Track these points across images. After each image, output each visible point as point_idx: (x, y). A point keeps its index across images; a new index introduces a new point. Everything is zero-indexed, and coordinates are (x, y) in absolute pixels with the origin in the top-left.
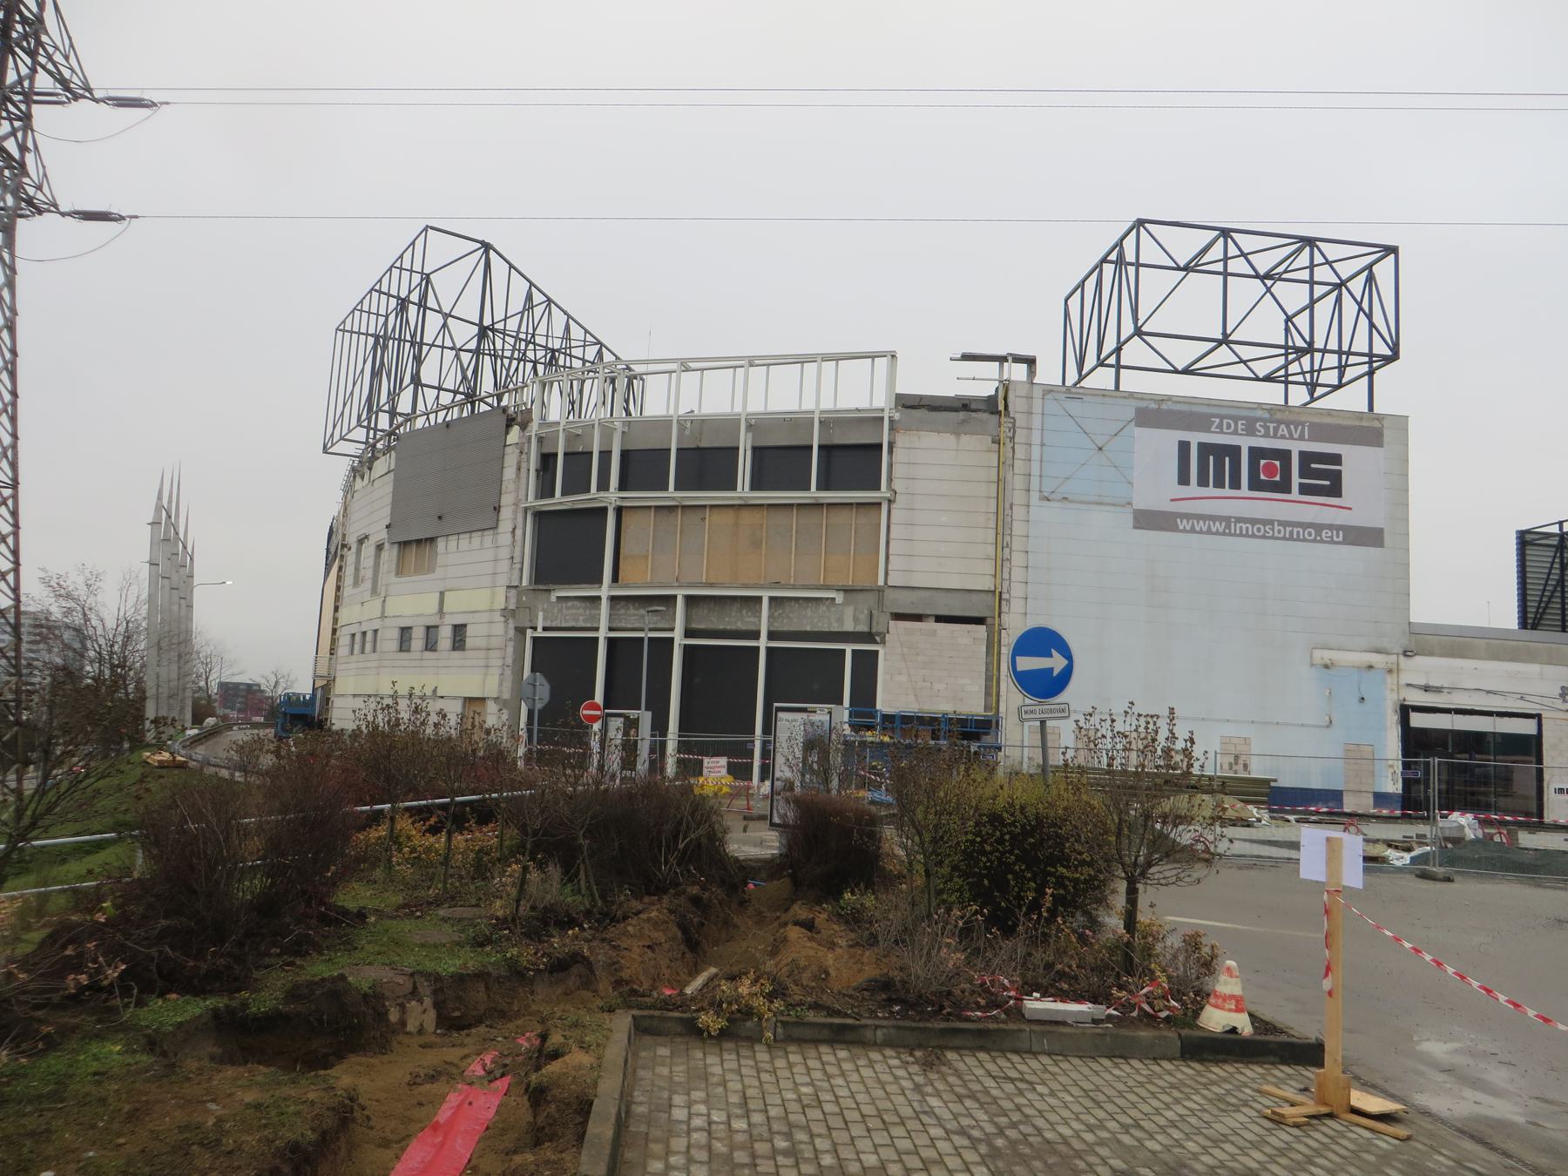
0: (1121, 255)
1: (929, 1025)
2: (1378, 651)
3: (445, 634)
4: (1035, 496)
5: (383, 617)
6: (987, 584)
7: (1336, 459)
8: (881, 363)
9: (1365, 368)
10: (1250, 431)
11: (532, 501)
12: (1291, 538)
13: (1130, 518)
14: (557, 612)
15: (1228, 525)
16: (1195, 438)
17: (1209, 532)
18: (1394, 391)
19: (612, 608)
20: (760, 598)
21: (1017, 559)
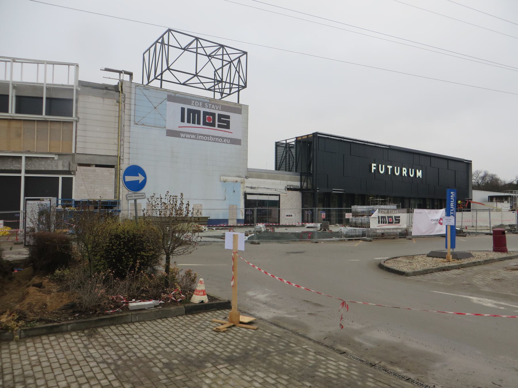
0: (163, 40)
1: (91, 319)
2: (239, 177)
4: (132, 123)
6: (115, 153)
7: (228, 117)
8: (72, 68)
9: (237, 89)
10: (204, 106)
12: (215, 141)
13: (165, 132)
15: (196, 136)
16: (186, 107)
17: (190, 138)
18: (245, 97)
20: (21, 157)
21: (126, 145)
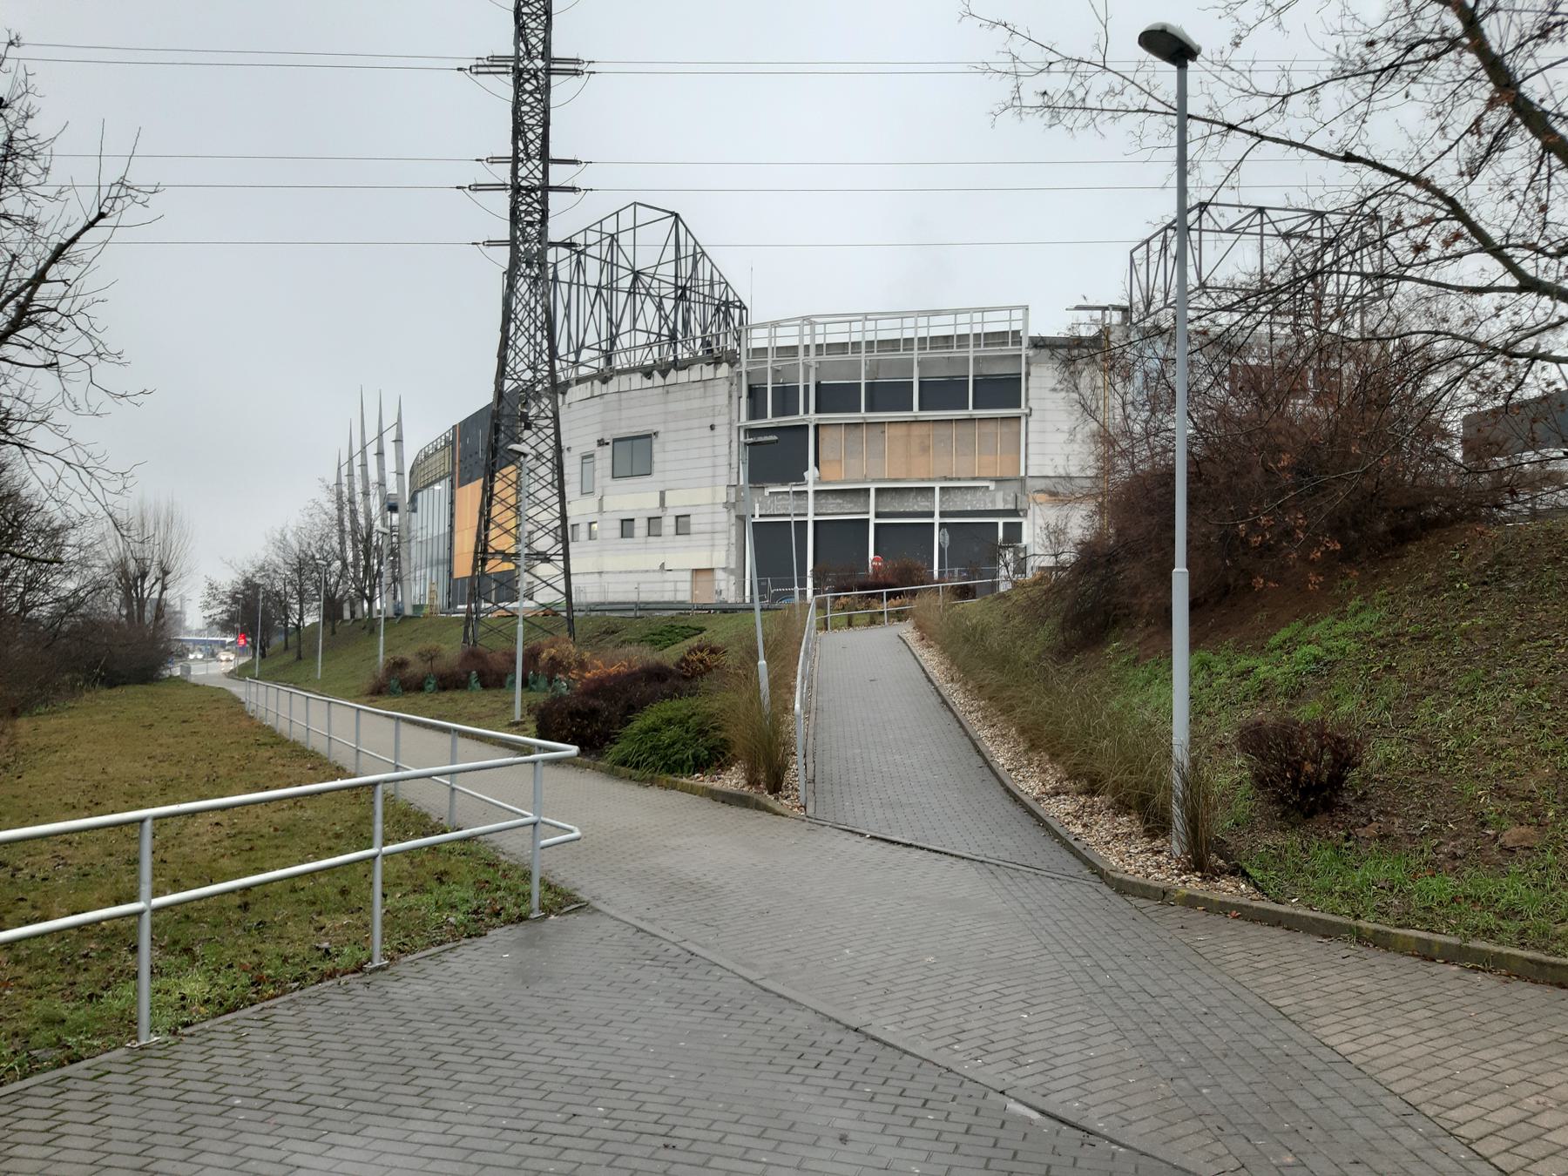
3: (668, 524)
5: (601, 511)
11: (744, 420)
14: (772, 503)
19: (815, 499)
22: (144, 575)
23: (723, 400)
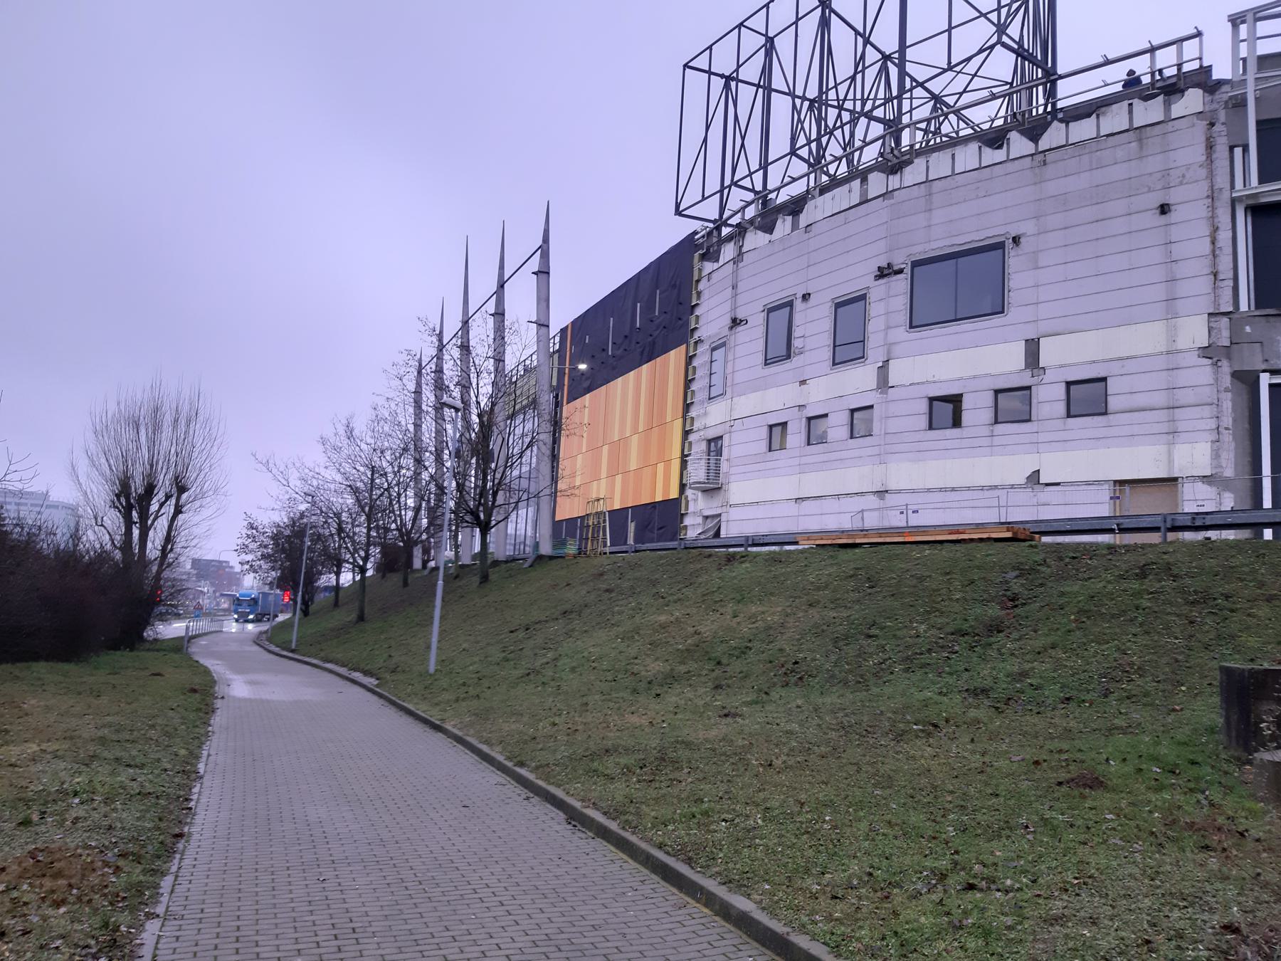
3: (1049, 397)
22: (150, 490)
23: (1198, 153)
